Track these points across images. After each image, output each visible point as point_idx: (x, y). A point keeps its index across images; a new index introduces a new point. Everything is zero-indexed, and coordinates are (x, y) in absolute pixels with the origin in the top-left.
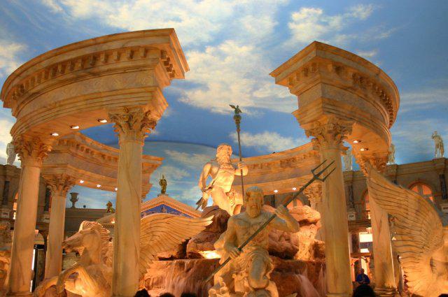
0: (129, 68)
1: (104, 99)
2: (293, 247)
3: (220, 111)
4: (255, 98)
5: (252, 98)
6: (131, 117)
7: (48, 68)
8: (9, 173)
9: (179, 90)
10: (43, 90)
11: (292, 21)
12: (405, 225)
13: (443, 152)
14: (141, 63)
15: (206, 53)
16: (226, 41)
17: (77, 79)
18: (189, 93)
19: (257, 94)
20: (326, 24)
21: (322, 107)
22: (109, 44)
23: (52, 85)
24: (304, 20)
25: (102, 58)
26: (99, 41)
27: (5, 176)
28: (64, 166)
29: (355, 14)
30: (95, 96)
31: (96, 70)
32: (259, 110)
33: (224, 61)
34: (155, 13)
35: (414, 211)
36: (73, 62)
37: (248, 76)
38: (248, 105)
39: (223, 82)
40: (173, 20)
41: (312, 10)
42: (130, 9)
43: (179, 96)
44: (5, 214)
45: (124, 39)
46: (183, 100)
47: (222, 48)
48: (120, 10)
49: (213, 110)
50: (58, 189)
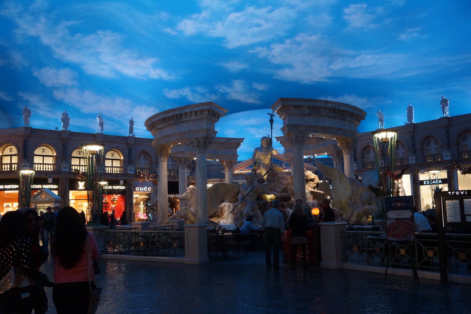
1: (187, 134)
2: (288, 196)
3: (307, 82)
6: (199, 142)
7: (162, 119)
10: (162, 127)
11: (345, 14)
12: (336, 185)
14: (200, 117)
15: (285, 44)
17: (175, 124)
18: (280, 72)
19: (332, 67)
20: (372, 13)
21: (288, 129)
23: (165, 126)
25: (184, 115)
26: (181, 108)
28: (183, 152)
30: (183, 133)
36: (173, 117)
38: (328, 75)
40: (255, 26)
41: (358, 5)
45: (191, 107)
46: (276, 77)
47: (297, 39)
48: (216, 26)
49: (301, 82)
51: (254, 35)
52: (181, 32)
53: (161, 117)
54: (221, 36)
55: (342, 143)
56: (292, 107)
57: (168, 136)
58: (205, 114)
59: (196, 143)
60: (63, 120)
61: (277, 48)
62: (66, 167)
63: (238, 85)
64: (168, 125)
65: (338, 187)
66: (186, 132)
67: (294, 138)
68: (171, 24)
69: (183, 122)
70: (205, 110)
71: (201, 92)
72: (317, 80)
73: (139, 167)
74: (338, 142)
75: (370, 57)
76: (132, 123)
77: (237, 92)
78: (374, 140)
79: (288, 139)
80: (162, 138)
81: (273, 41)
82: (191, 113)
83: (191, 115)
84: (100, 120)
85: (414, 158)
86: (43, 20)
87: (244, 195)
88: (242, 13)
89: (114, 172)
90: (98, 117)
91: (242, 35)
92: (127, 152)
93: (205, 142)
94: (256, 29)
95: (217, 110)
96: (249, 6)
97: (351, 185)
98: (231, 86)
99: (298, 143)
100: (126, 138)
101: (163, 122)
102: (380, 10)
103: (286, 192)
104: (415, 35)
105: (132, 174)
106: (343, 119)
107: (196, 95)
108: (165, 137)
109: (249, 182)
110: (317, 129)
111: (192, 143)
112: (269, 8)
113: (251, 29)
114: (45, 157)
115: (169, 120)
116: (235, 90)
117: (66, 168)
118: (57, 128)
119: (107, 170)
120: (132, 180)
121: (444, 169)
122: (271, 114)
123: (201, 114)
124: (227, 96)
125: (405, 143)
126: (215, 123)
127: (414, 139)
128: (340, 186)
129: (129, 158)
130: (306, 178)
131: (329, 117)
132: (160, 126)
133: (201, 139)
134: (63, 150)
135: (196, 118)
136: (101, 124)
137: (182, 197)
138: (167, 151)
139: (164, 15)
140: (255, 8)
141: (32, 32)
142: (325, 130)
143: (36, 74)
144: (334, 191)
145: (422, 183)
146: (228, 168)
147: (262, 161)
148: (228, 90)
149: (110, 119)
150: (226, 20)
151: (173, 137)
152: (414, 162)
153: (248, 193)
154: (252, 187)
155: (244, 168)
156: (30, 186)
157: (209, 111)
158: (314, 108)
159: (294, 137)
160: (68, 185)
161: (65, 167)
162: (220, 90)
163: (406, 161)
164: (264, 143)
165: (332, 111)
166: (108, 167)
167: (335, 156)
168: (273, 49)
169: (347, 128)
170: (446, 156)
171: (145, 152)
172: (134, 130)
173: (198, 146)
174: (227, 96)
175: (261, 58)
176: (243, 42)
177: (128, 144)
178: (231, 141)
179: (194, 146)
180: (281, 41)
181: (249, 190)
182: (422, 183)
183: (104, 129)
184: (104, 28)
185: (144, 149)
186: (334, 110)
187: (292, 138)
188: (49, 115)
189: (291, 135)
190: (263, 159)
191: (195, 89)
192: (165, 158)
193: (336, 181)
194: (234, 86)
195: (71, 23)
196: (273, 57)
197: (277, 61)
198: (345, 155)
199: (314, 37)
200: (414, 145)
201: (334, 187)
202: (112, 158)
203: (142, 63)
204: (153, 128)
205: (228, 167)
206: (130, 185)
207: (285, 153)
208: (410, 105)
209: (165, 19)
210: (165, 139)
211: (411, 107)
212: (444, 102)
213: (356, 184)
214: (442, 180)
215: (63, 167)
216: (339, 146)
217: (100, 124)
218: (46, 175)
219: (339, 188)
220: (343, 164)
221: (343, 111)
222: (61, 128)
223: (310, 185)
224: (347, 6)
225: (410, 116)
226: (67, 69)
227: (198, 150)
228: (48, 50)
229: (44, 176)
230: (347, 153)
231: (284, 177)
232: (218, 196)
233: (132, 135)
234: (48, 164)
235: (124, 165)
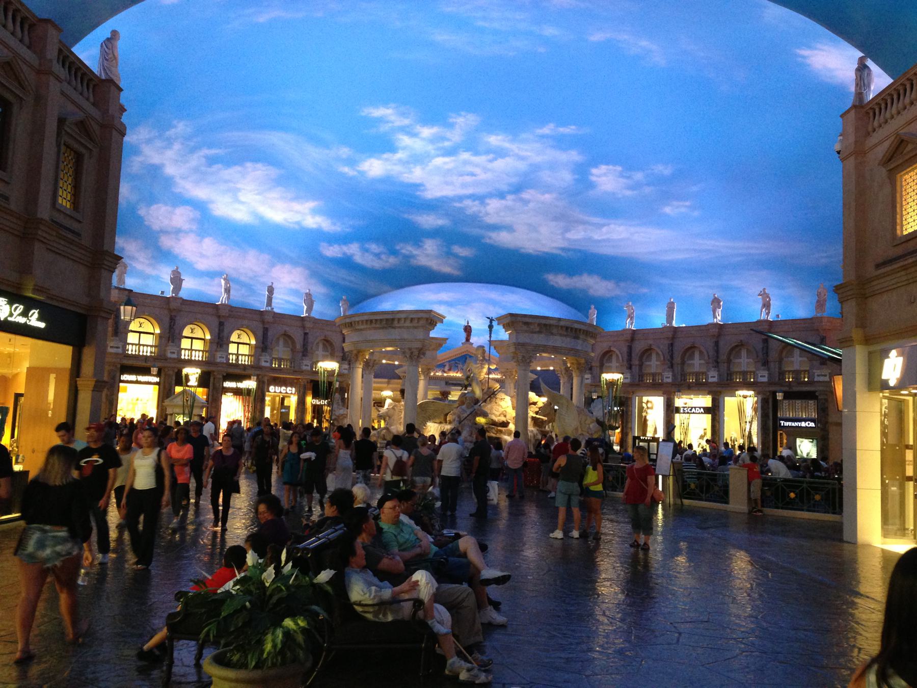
3: (531, 251)
4: (569, 240)
5: (564, 239)
6: (412, 353)
8: (308, 325)
9: (482, 232)
13: (768, 314)
14: (416, 325)
16: (529, 191)
17: (383, 328)
18: (494, 235)
19: (568, 235)
20: (628, 178)
24: (605, 174)
27: (304, 327)
29: (656, 171)
31: (393, 326)
32: (575, 250)
33: (527, 206)
34: (449, 170)
37: (556, 219)
38: (563, 246)
39: (529, 225)
40: (468, 175)
41: (611, 167)
42: (423, 169)
43: (483, 237)
44: (306, 365)
46: (488, 241)
48: (413, 170)
49: (523, 250)
51: (464, 185)
52: (362, 173)
54: (418, 182)
55: (572, 363)
56: (521, 323)
58: (422, 322)
60: (173, 281)
61: (494, 205)
62: (174, 351)
63: (430, 245)
68: (351, 162)
71: (375, 251)
72: (546, 250)
75: (621, 228)
76: (271, 290)
77: (427, 255)
78: (602, 379)
81: (491, 195)
82: (405, 319)
83: (405, 321)
84: (226, 284)
85: (670, 374)
86: (177, 146)
88: (453, 158)
89: (240, 362)
90: (224, 279)
91: (447, 183)
94: (468, 179)
96: (464, 151)
97: (579, 414)
100: (261, 313)
102: (639, 176)
103: (505, 416)
104: (683, 210)
106: (576, 338)
107: (367, 254)
110: (545, 349)
112: (491, 156)
113: (461, 178)
114: (142, 335)
116: (425, 252)
117: (174, 353)
118: (163, 293)
119: (231, 359)
121: (709, 394)
123: (418, 322)
124: (412, 260)
125: (660, 353)
127: (672, 348)
131: (561, 335)
132: (362, 327)
134: (170, 326)
136: (228, 291)
139: (345, 152)
140: (471, 155)
141: (156, 159)
142: (555, 350)
143: (142, 212)
145: (677, 410)
148: (415, 252)
149: (238, 282)
150: (430, 164)
152: (670, 380)
154: (471, 410)
156: (120, 376)
157: (427, 319)
158: (545, 325)
160: (174, 378)
161: (172, 351)
162: (403, 251)
163: (660, 377)
165: (564, 329)
166: (233, 354)
168: (488, 204)
169: (579, 348)
170: (711, 377)
171: (286, 336)
172: (273, 300)
174: (412, 260)
175: (469, 214)
176: (448, 192)
177: (263, 322)
180: (501, 195)
181: (468, 413)
182: (677, 410)
183: (231, 297)
184: (256, 160)
185: (285, 331)
186: (567, 328)
188: (149, 271)
191: (367, 246)
192: (360, 364)
194: (425, 247)
195: (213, 151)
196: (487, 214)
197: (491, 220)
199: (547, 196)
200: (672, 357)
203: (297, 206)
208: (672, 300)
209: (344, 156)
211: (673, 303)
212: (716, 302)
214: (704, 408)
215: (169, 351)
217: (226, 290)
218: (146, 362)
220: (572, 385)
221: (576, 329)
222: (169, 294)
223: (532, 409)
224: (596, 166)
225: (670, 317)
226: (188, 207)
228: (169, 182)
229: (143, 364)
234: (147, 346)
235: (256, 351)
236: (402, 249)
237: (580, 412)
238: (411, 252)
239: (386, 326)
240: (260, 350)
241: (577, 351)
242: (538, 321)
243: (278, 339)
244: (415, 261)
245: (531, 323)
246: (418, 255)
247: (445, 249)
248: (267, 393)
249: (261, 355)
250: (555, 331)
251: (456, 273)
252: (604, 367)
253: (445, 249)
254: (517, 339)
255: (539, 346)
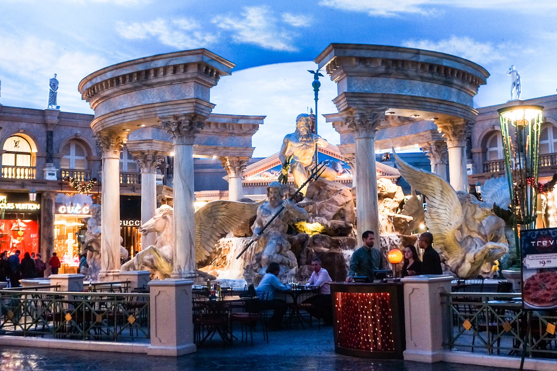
0: (174, 81)
1: (158, 109)
2: (346, 225)
3: (382, 13)
6: (179, 124)
7: (112, 79)
14: (183, 76)
17: (135, 89)
21: (347, 100)
22: (155, 62)
25: (152, 72)
26: (147, 59)
28: (150, 141)
30: (150, 106)
31: (149, 82)
35: (439, 192)
36: (131, 75)
50: (146, 166)
53: (109, 75)
55: (445, 127)
56: (354, 59)
57: (123, 111)
58: (193, 71)
59: (174, 125)
64: (123, 90)
65: (438, 208)
66: (156, 105)
67: (358, 118)
69: (151, 86)
70: (194, 63)
73: (67, 168)
74: (439, 126)
76: (54, 84)
77: (253, 29)
79: (347, 120)
80: (111, 114)
82: (166, 68)
83: (165, 74)
87: (264, 224)
92: (44, 138)
93: (191, 124)
95: (214, 64)
97: (462, 205)
98: (242, 18)
99: (365, 127)
100: (42, 113)
101: (112, 86)
103: (343, 218)
105: (53, 182)
106: (449, 84)
107: (176, 33)
108: (117, 113)
109: (273, 199)
111: (167, 124)
115: (124, 82)
116: (249, 25)
120: (53, 192)
122: (316, 72)
123: (185, 71)
126: (210, 88)
128: (440, 207)
129: (47, 151)
130: (378, 192)
131: (423, 79)
132: (107, 92)
133: (183, 118)
135: (174, 78)
137: (146, 227)
138: (120, 138)
144: (430, 216)
146: (235, 172)
147: (298, 159)
148: (238, 26)
151: (131, 113)
153: (272, 220)
154: (278, 209)
155: (265, 170)
157: (199, 65)
158: (395, 62)
159: (358, 115)
162: (222, 26)
164: (302, 125)
165: (427, 68)
167: (433, 150)
169: (454, 99)
171: (77, 140)
173: (178, 130)
174: (234, 37)
177: (46, 124)
178: (241, 122)
179: (170, 131)
181: (273, 215)
185: (76, 135)
186: (431, 66)
187: (354, 118)
189: (351, 113)
190: (300, 156)
191: (175, 22)
193: (434, 198)
194: (248, 18)
198: (450, 149)
201: (431, 209)
202: (16, 150)
204: (93, 96)
205: (234, 170)
206: (50, 201)
207: (341, 145)
210: (116, 117)
213: (471, 203)
216: (440, 132)
219: (439, 211)
221: (446, 68)
223: (387, 204)
227: (177, 137)
230: (455, 145)
231: (339, 190)
232: (214, 226)
233: (54, 107)
236: (218, 23)
237: (463, 198)
238: (231, 25)
239: (138, 84)
240: (44, 160)
241: (450, 104)
242: (382, 54)
243: (68, 146)
244: (239, 38)
245: (371, 59)
246: (241, 30)
247: (274, 20)
248: (56, 216)
249: (45, 167)
250: (411, 72)
251: (291, 49)
252: (488, 153)
253: (274, 20)
254: (349, 86)
255: (388, 96)
